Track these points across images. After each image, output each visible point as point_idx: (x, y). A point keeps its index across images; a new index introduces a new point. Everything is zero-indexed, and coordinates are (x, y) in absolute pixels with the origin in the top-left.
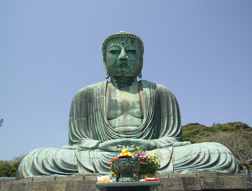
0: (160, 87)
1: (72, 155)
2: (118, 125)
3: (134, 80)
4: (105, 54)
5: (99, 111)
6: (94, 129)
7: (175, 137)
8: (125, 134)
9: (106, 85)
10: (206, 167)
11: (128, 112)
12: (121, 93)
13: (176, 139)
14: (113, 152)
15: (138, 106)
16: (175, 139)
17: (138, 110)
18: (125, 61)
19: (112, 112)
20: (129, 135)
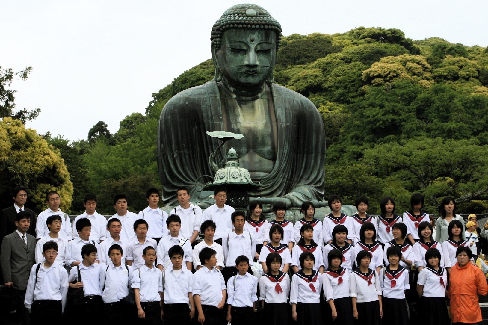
7: (315, 184)
9: (220, 100)
13: (316, 187)
15: (268, 141)
16: (314, 189)
17: (268, 148)
18: (254, 69)
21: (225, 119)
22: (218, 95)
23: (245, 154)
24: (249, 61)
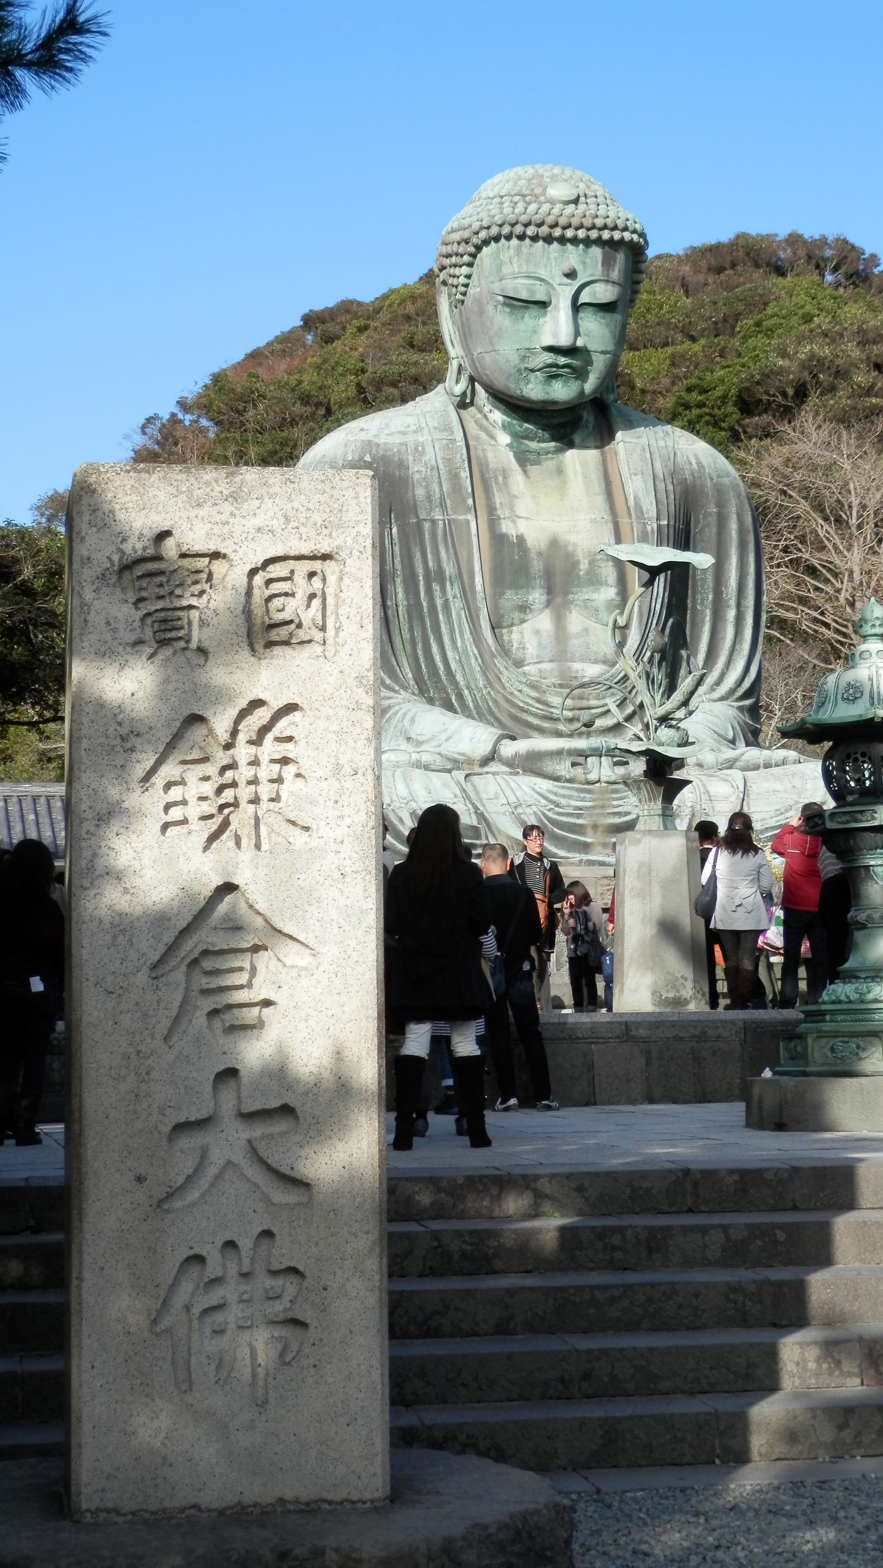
0: (695, 466)
1: (456, 796)
2: (535, 653)
4: (466, 286)
5: (452, 584)
6: (420, 653)
11: (571, 596)
12: (533, 497)
13: (741, 709)
14: (557, 779)
16: (736, 712)
17: (610, 593)
19: (510, 598)
20: (581, 698)
22: (459, 435)
23: (541, 611)
24: (555, 335)
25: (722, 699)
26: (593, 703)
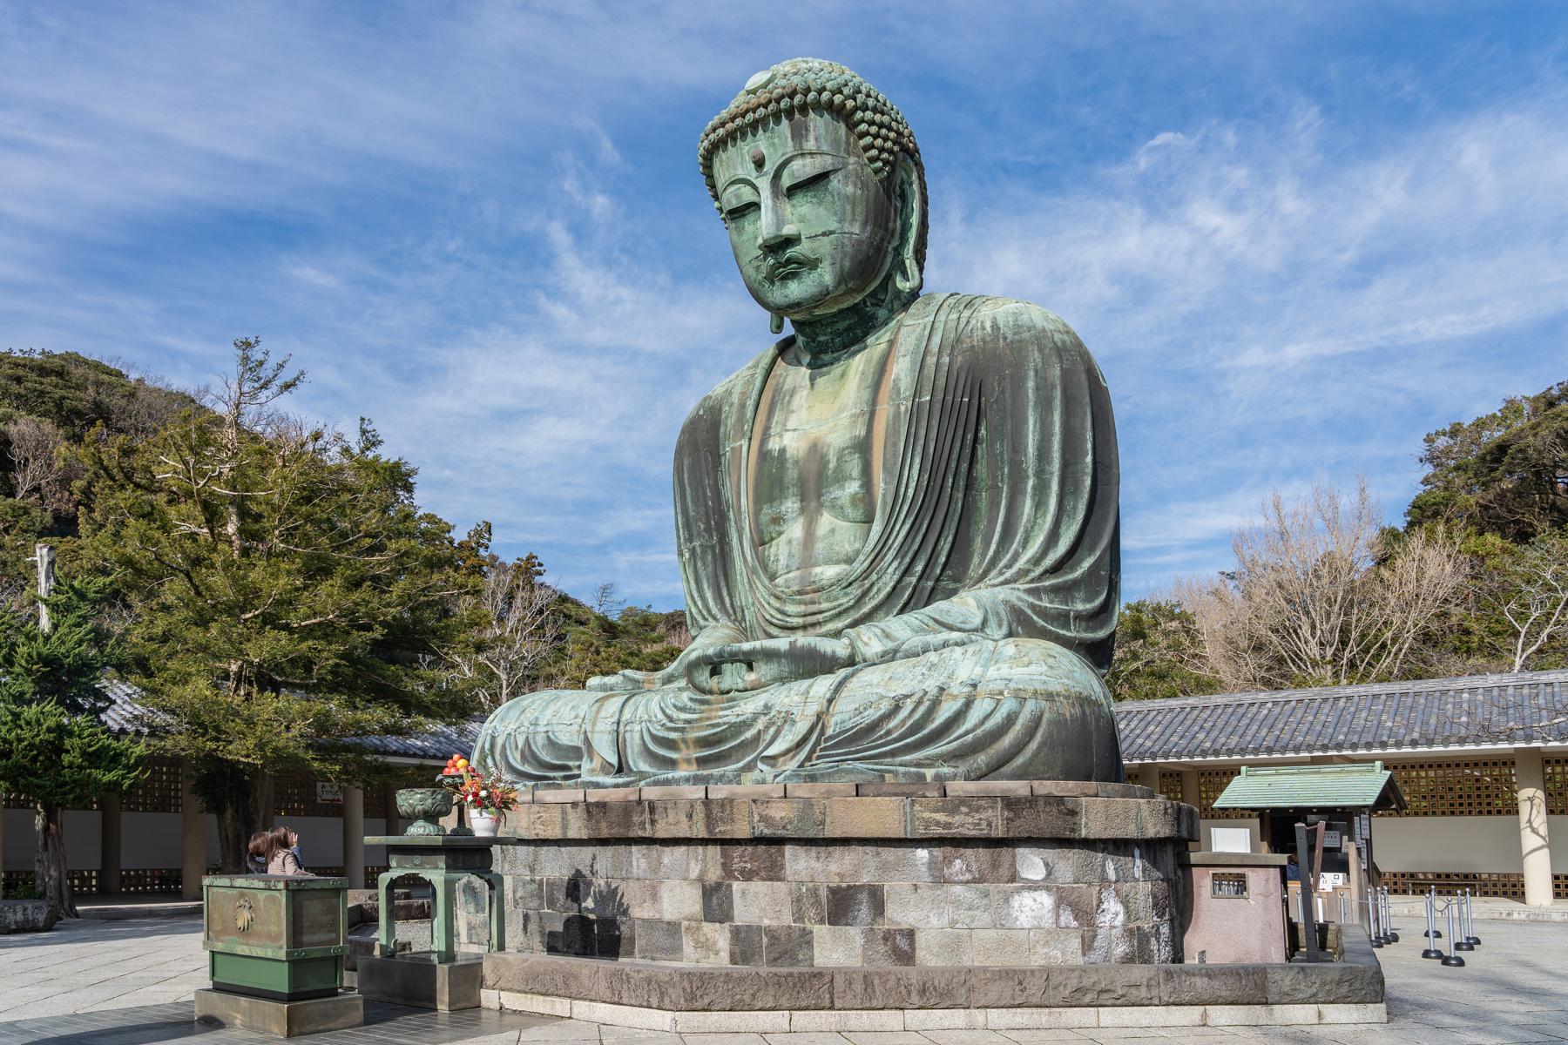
3: (873, 317)
7: (1032, 581)
8: (800, 603)
10: (893, 754)
15: (854, 465)
17: (854, 487)
19: (767, 512)
20: (813, 603)
21: (758, 429)
25: (1002, 584)
26: (825, 606)
